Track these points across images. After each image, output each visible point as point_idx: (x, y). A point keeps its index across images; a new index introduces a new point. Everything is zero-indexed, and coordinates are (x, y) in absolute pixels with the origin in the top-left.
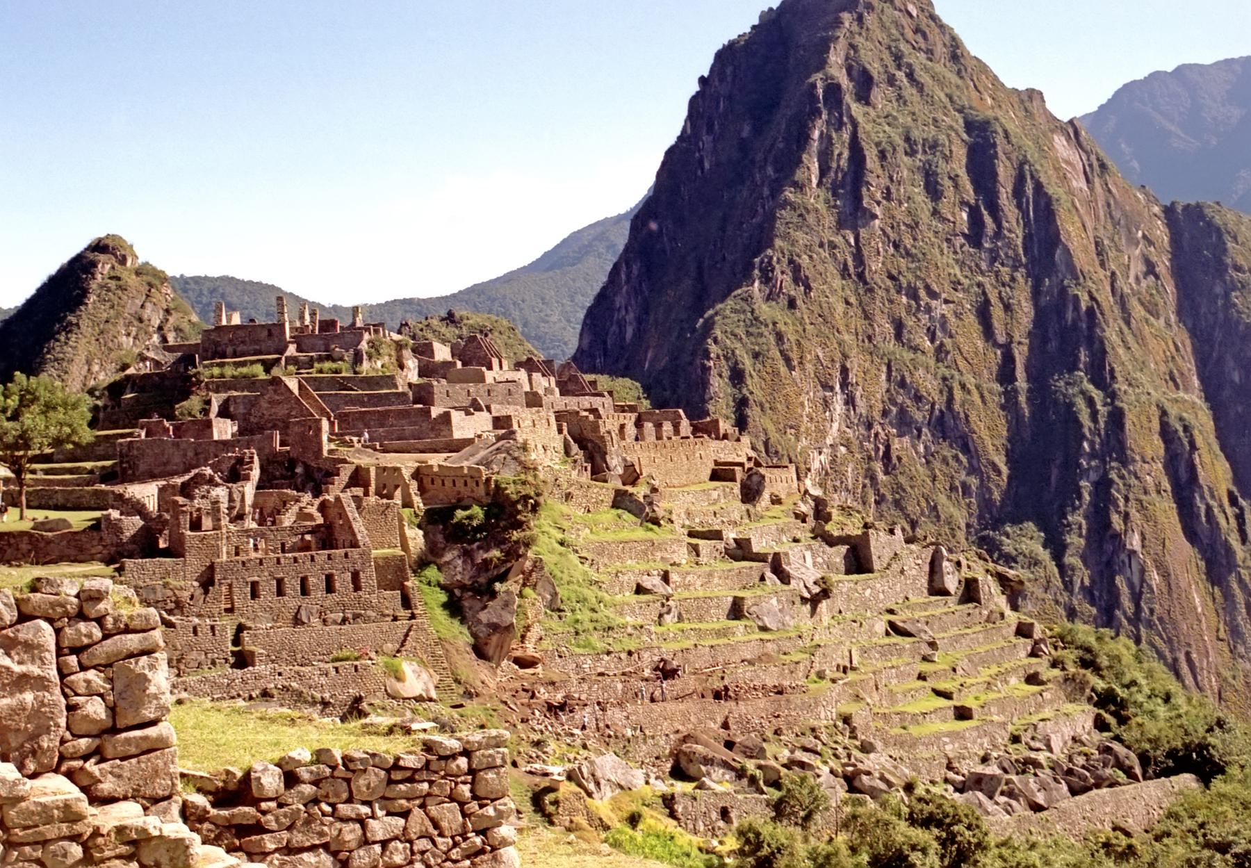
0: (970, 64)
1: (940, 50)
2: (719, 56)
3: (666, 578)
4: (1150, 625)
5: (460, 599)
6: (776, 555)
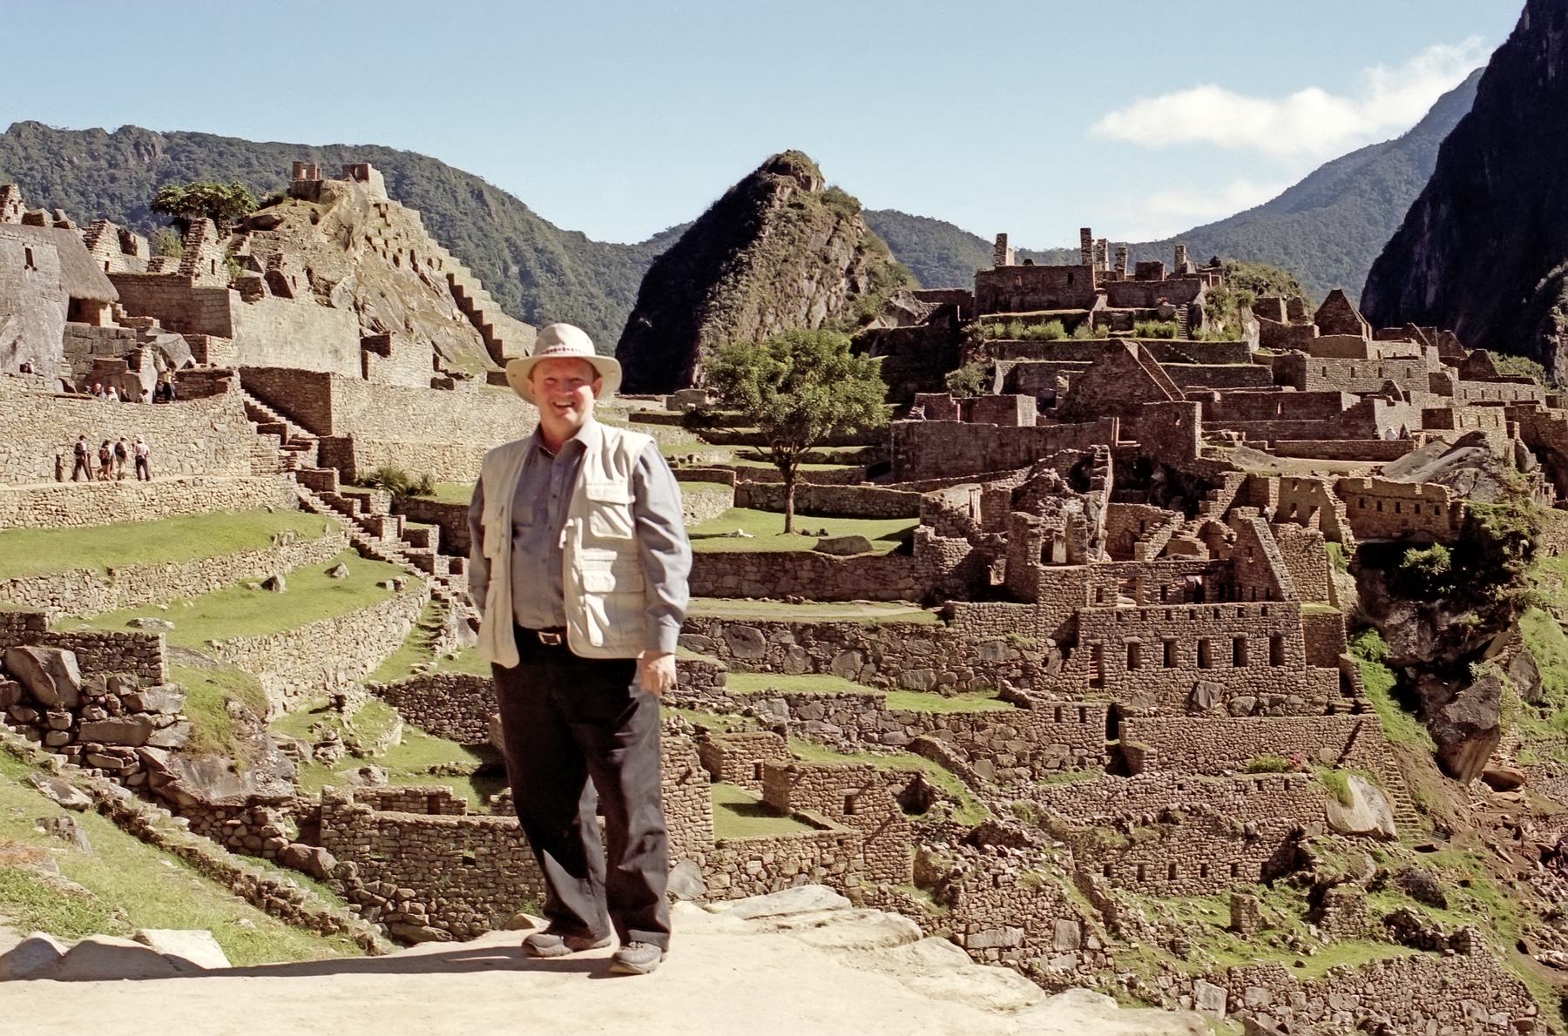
5: (1415, 682)
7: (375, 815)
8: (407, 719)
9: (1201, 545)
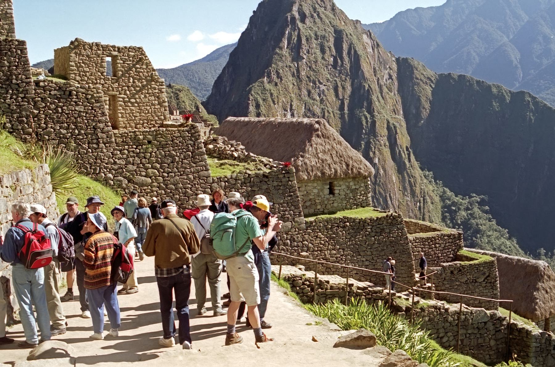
0: (337, 11)
1: (329, 7)
2: (260, 5)
4: (379, 185)
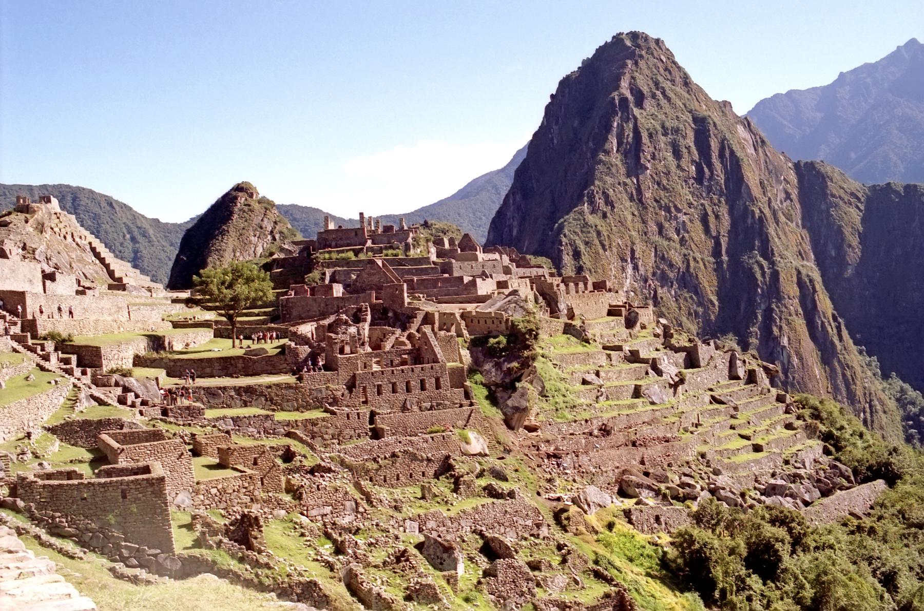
0: (694, 87)
2: (561, 83)
3: (597, 374)
6: (654, 359)
7: (40, 482)
8: (61, 440)
9: (407, 342)
